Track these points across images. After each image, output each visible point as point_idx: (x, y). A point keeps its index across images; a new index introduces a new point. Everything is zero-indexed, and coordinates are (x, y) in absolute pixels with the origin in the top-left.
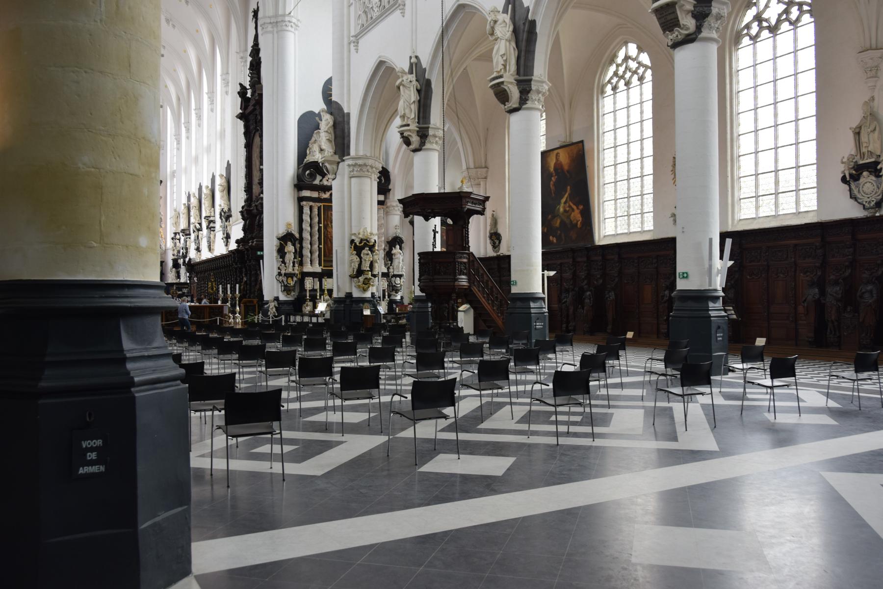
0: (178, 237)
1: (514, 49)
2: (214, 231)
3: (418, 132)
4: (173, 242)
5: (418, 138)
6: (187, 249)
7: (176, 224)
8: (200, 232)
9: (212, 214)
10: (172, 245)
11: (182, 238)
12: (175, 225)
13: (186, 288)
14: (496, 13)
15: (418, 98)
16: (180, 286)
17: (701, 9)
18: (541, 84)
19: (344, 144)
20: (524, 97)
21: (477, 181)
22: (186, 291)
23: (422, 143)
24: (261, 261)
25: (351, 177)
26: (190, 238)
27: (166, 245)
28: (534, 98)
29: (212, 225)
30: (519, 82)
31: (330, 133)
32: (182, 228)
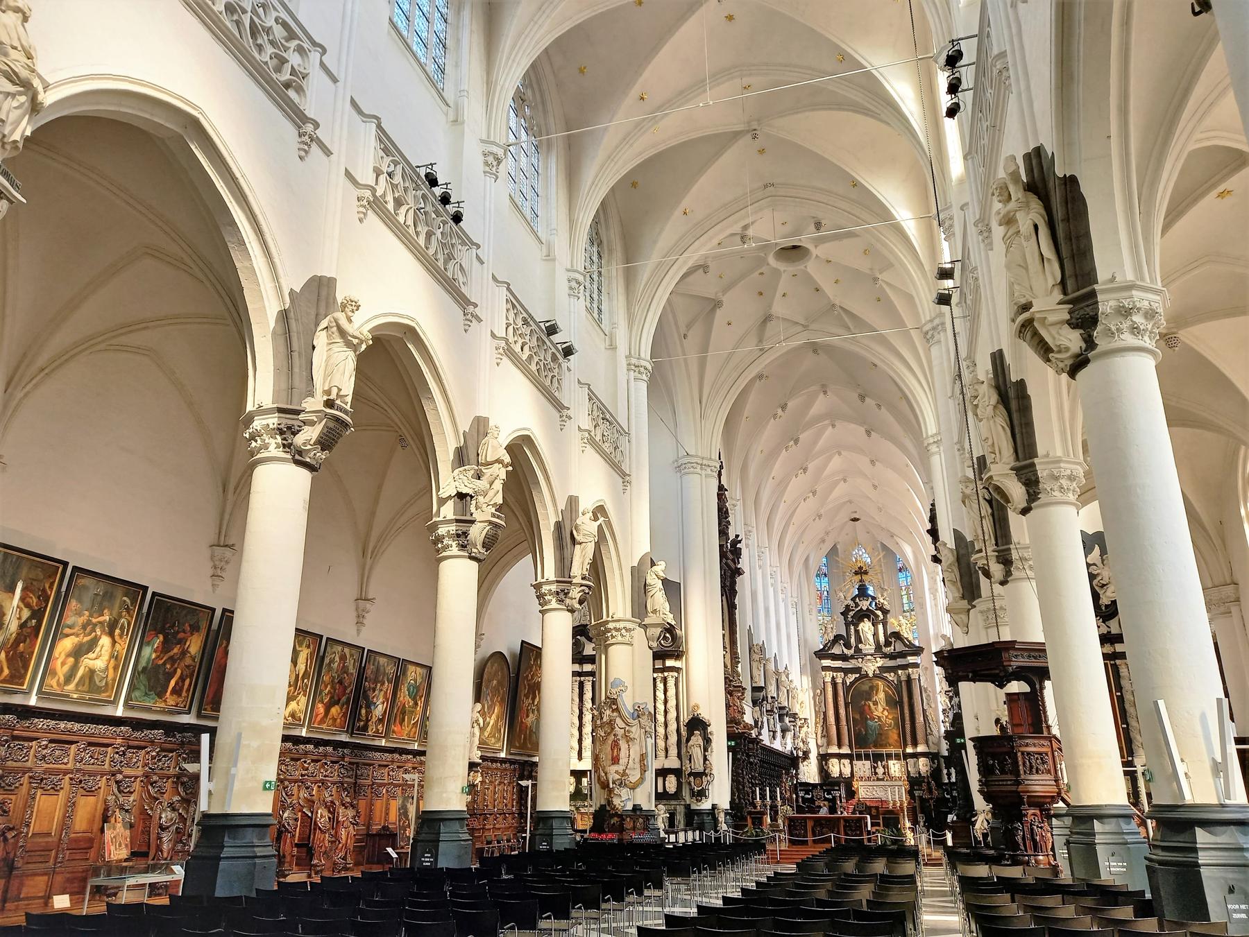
1: (1003, 427)
3: (997, 556)
5: (1002, 566)
14: (976, 387)
15: (990, 511)
17: (1082, 312)
18: (1057, 465)
19: (972, 583)
20: (1031, 491)
21: (1222, 609)
23: (1008, 573)
24: (963, 751)
25: (987, 628)
27: (939, 731)
28: (1048, 489)
30: (1018, 471)
31: (953, 571)
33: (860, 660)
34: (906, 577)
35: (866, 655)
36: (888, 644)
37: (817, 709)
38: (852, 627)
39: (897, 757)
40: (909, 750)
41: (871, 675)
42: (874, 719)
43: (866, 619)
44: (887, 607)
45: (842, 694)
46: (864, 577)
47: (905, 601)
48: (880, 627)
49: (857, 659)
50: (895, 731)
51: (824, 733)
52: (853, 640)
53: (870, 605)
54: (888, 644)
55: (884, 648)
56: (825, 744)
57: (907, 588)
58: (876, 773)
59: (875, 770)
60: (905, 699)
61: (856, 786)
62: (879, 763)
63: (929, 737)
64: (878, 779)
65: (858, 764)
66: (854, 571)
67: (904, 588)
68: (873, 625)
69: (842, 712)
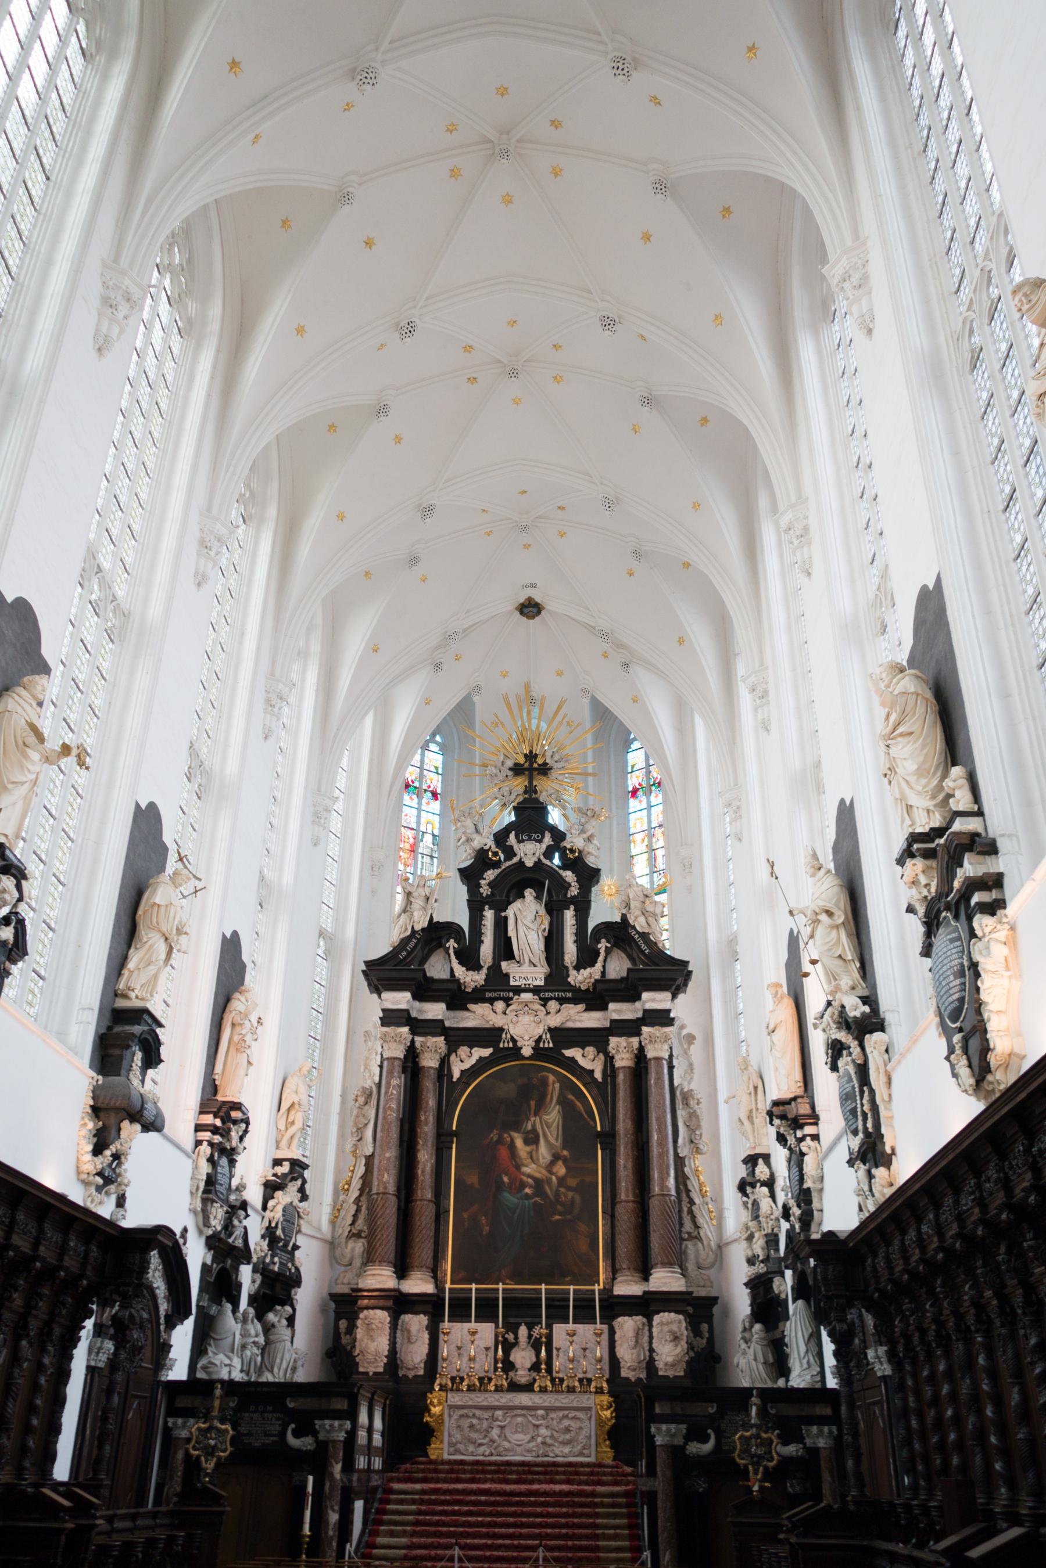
0: (762, 1171)
2: (992, 908)
4: (745, 1204)
6: (804, 1197)
7: (750, 1118)
8: (874, 1041)
9: (962, 801)
10: (745, 1216)
11: (780, 1156)
12: (746, 1122)
13: (821, 1421)
16: (789, 1410)
22: (822, 1443)
26: (816, 1137)
27: (720, 1227)
29: (971, 867)
32: (775, 1098)
33: (500, 1005)
34: (650, 807)
35: (518, 990)
36: (587, 958)
37: (349, 1147)
38: (489, 915)
39: (584, 1312)
40: (628, 1287)
41: (527, 1051)
42: (523, 1185)
43: (529, 893)
44: (591, 861)
45: (430, 1101)
46: (540, 783)
47: (641, 867)
48: (569, 916)
49: (491, 1001)
50: (582, 1227)
51: (361, 1224)
52: (487, 950)
53: (548, 854)
54: (587, 958)
55: (573, 972)
56: (358, 1262)
57: (650, 834)
58: (509, 1366)
59: (507, 1352)
60: (624, 1124)
61: (436, 1410)
62: (523, 1331)
63: (690, 1247)
64: (515, 1387)
65: (455, 1332)
66: (510, 763)
67: (638, 837)
68: (549, 910)
69: (425, 1157)
